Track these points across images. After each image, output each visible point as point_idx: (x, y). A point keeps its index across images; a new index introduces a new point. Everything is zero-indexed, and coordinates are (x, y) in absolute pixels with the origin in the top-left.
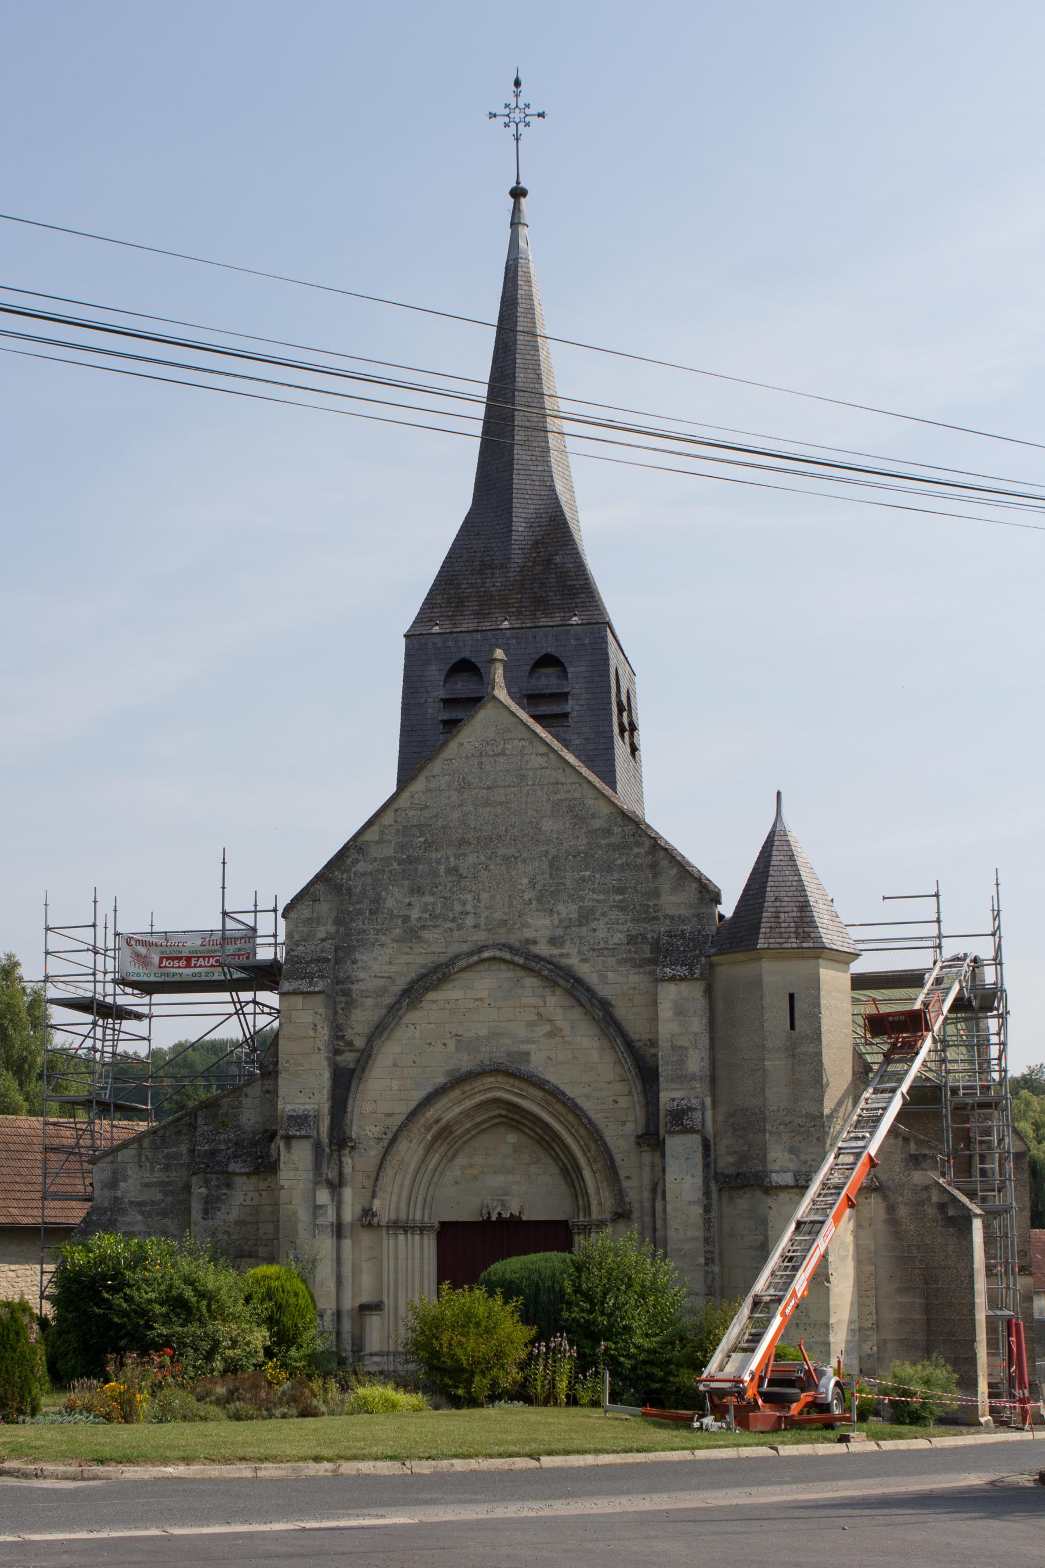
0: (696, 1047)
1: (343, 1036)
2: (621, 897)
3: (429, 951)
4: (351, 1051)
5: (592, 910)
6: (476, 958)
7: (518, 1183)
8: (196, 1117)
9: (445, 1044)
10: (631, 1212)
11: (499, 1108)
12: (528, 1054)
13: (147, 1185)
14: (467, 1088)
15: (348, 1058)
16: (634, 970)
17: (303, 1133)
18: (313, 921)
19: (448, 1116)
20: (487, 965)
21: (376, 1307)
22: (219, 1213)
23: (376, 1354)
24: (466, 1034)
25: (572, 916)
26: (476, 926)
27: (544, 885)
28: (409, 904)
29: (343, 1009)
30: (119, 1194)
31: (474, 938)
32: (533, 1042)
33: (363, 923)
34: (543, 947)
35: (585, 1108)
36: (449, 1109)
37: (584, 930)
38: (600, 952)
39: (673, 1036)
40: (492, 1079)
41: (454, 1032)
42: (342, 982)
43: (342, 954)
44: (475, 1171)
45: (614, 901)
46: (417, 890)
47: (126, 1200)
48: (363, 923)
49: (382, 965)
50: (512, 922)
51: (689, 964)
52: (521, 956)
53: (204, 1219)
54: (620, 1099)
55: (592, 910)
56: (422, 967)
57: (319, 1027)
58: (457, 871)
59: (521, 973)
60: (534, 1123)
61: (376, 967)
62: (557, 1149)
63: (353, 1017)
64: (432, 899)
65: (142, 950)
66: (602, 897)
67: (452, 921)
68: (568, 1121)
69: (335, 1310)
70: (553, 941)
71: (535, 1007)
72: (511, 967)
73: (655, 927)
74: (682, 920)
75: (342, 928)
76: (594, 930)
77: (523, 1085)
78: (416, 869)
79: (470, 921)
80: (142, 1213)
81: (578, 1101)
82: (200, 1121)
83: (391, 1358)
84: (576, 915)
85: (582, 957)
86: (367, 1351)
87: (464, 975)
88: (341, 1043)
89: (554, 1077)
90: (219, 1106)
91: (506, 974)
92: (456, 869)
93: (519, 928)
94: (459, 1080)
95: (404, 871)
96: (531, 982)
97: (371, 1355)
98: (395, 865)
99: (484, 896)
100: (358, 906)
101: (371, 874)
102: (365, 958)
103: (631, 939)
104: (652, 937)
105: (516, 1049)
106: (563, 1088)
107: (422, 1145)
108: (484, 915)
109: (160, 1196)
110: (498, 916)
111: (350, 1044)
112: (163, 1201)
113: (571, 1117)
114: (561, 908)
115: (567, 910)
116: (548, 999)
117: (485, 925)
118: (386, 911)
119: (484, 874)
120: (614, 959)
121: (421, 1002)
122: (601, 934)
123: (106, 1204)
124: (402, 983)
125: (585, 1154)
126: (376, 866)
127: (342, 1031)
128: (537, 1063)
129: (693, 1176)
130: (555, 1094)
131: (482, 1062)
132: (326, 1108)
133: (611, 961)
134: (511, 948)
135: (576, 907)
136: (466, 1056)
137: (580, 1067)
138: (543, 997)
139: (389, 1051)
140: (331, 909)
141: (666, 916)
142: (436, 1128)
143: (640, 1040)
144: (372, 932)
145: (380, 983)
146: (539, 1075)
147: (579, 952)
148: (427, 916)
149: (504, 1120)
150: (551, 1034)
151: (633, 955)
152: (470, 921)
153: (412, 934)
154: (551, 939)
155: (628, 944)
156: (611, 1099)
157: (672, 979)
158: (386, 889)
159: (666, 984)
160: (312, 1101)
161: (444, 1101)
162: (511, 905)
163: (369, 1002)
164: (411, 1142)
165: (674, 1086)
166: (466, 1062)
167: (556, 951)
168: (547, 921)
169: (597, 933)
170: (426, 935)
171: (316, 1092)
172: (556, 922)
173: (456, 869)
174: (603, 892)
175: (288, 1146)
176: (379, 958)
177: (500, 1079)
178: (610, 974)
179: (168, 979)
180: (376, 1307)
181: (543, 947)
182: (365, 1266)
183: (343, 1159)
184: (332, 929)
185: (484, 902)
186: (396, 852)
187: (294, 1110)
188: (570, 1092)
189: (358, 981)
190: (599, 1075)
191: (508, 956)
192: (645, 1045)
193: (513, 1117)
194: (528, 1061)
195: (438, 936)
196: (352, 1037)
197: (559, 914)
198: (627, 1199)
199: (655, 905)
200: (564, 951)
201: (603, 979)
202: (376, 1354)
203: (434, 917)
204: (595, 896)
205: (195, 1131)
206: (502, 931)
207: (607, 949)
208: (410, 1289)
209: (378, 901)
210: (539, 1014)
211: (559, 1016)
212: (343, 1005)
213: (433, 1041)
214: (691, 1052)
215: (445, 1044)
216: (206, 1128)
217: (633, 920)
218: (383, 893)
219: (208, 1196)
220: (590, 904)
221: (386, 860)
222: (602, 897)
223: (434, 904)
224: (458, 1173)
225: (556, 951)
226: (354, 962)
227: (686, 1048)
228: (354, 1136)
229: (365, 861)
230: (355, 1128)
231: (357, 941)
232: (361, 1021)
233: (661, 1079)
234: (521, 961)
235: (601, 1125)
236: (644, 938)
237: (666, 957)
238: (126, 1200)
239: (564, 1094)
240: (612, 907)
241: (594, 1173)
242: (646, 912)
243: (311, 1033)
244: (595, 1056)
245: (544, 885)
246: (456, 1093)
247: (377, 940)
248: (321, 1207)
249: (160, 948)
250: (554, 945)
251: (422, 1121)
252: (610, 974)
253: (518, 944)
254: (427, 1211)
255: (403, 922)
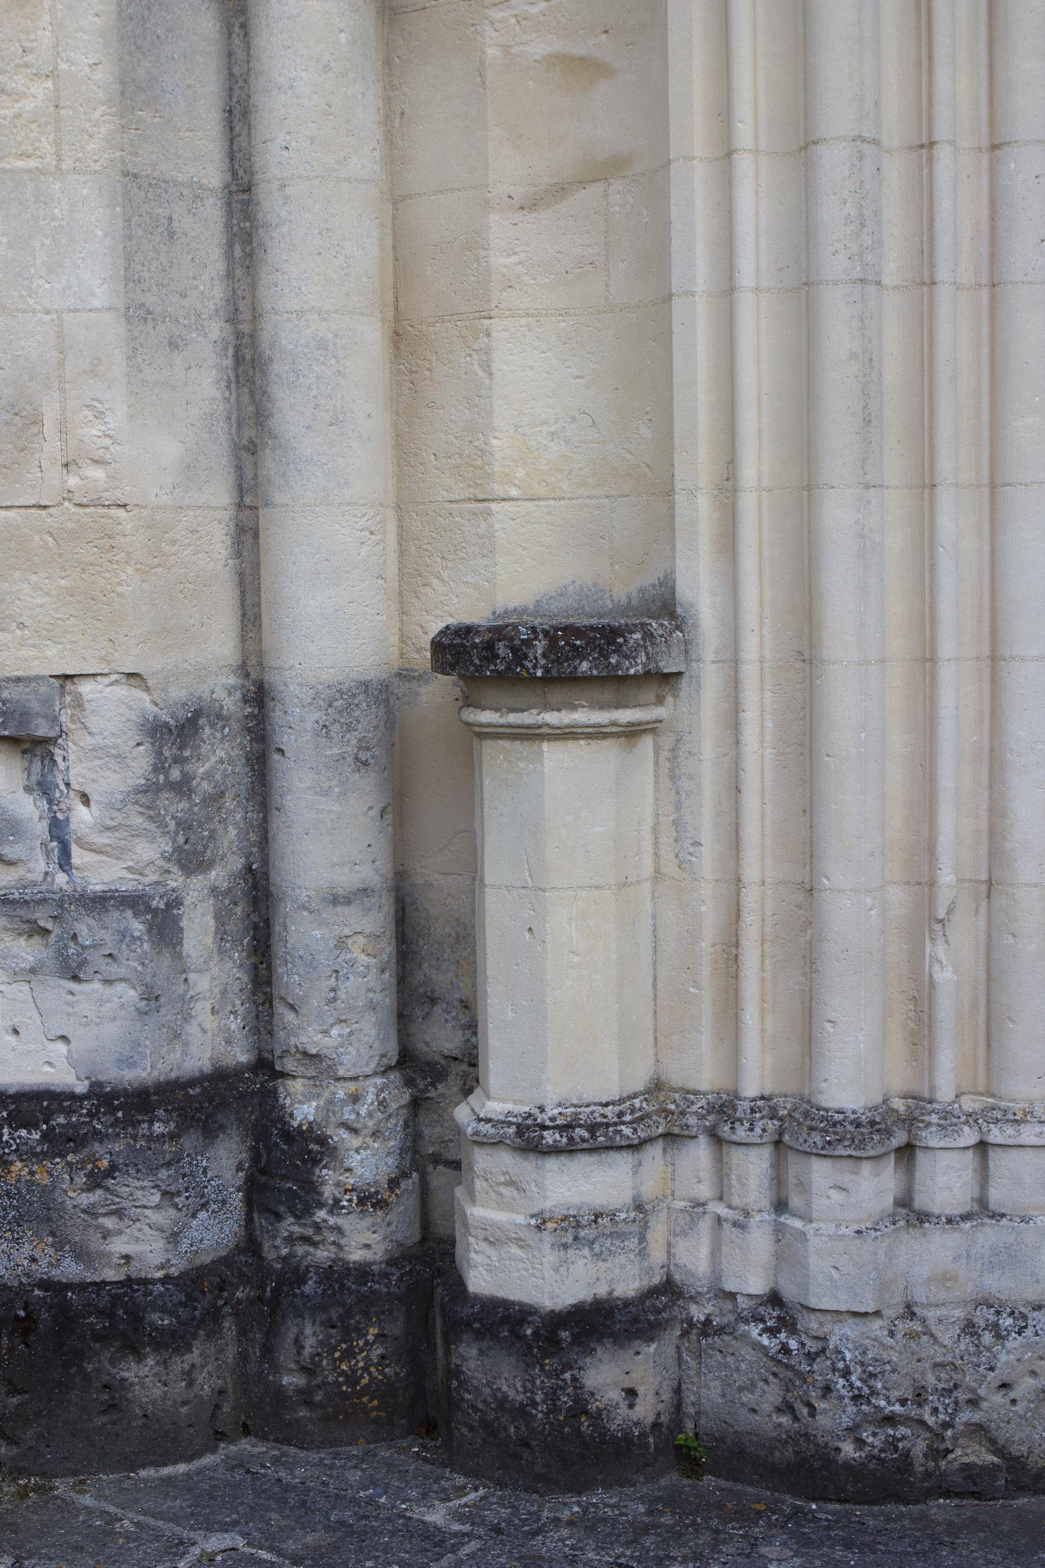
21: (587, 659)
23: (584, 1135)
69: (222, 689)
83: (753, 1167)
86: (500, 1098)
97: (530, 1138)
180: (587, 659)
182: (514, 246)
202: (584, 1135)
208: (956, 460)
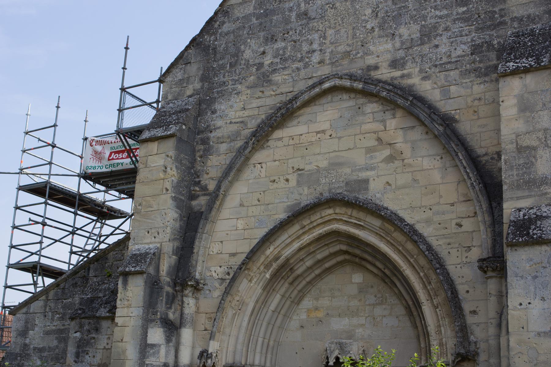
0: (547, 146)
1: (200, 181)
2: (465, 9)
3: (278, 92)
4: (205, 195)
5: (435, 27)
6: (317, 90)
7: (362, 325)
8: (89, 270)
9: (287, 180)
10: (477, 354)
11: (341, 242)
12: (366, 181)
13: (47, 333)
14: (306, 222)
15: (201, 202)
16: (479, 80)
17: (138, 268)
18: (183, 82)
19: (288, 252)
20: (329, 97)
22: (87, 357)
24: (307, 168)
25: (414, 36)
26: (321, 62)
27: (387, 12)
28: (264, 53)
29: (201, 157)
30: (27, 341)
31: (319, 73)
32: (372, 169)
33: (224, 77)
34: (384, 71)
35: (425, 234)
36: (287, 246)
37: (426, 48)
38: (443, 67)
39: (518, 136)
40: (330, 211)
41: (296, 167)
42: (202, 132)
43: (205, 106)
44: (320, 314)
45: (458, 14)
46: (272, 39)
47: (32, 347)
48: (224, 77)
49: (237, 112)
50: (354, 52)
51: (537, 55)
52: (360, 81)
53: (75, 362)
54: (465, 222)
55: (435, 27)
56: (271, 109)
57: (168, 169)
58: (306, 15)
59: (362, 100)
60: (375, 257)
61: (232, 114)
62: (398, 284)
63: (209, 163)
64: (283, 44)
65: (99, 148)
66: (445, 12)
67: (300, 61)
68: (407, 251)
70: (395, 64)
71: (375, 132)
72: (353, 95)
73: (501, 32)
74: (531, 19)
75: (206, 84)
76: (437, 46)
77: (361, 215)
78: (271, 21)
79: (316, 58)
80: (41, 358)
81: (418, 227)
82: (92, 273)
84: (418, 35)
85: (424, 75)
87: (308, 110)
88: (197, 189)
89: (392, 203)
90: (107, 259)
91: (346, 103)
92: (306, 14)
93: (361, 57)
94: (298, 214)
95: (261, 24)
96: (372, 107)
98: (254, 20)
99: (330, 32)
100: (221, 62)
101: (233, 32)
102: (223, 107)
103: (476, 49)
104: (499, 43)
105: (355, 178)
106: (401, 214)
107: (261, 284)
108: (328, 50)
109: (55, 343)
110: (342, 48)
111: (204, 188)
112: (57, 346)
113: (410, 246)
114: (404, 31)
115: (409, 31)
116: (388, 123)
117: (330, 59)
118: (243, 62)
119: (330, 13)
120: (457, 72)
121: (268, 141)
122: (443, 49)
123: (18, 350)
124: (253, 125)
125: (425, 287)
126: (238, 24)
127: (198, 177)
128: (377, 191)
129: (543, 299)
130: (391, 220)
131: (321, 194)
132: (168, 248)
133: (454, 74)
134: (352, 77)
135: (418, 27)
136: (306, 191)
137: (420, 189)
138: (383, 121)
139: (239, 191)
140: (199, 69)
141: (513, 20)
142: (275, 266)
143: (486, 154)
144: (230, 83)
145: (234, 127)
146: (378, 202)
147: (421, 71)
148: (278, 60)
149: (347, 257)
150: (391, 159)
151: (477, 65)
152: (316, 58)
153: (265, 79)
154: (393, 62)
155: (472, 54)
156: (454, 222)
157: (515, 72)
158: (245, 43)
159: (508, 79)
160: (157, 240)
161: (284, 237)
162: (354, 36)
163: (223, 147)
164: (250, 281)
165: (520, 193)
166: (306, 196)
167: (398, 73)
168: (389, 46)
169: (440, 49)
170: (277, 78)
171: (161, 231)
172: (398, 45)
173: (306, 14)
174: (445, 7)
175: (125, 283)
176: (235, 105)
177: (338, 211)
178: (453, 88)
179: (114, 169)
181: (384, 71)
183: (185, 299)
184: (198, 85)
185: (329, 39)
186: (255, 8)
187: (139, 250)
188: (409, 218)
189: (215, 129)
190: (441, 197)
191: (347, 83)
192: (492, 159)
193: (356, 254)
194: (367, 189)
195: (286, 77)
196: (207, 182)
197: (400, 36)
198: (472, 338)
199: (501, 10)
200: (405, 72)
201: (446, 95)
203: (284, 60)
204: (438, 13)
205: (87, 283)
206: (345, 62)
207: (449, 62)
209: (237, 54)
210: (379, 140)
211: (399, 138)
212: (201, 153)
213: (276, 178)
214: (540, 152)
215: (287, 180)
216: (95, 279)
217: (477, 29)
218: (242, 47)
219: (80, 340)
220: (433, 21)
221: (247, 18)
222: (445, 12)
223: (285, 48)
224: (304, 316)
225: (398, 73)
226: (214, 112)
227: (535, 149)
228: (197, 276)
229: (229, 22)
230: (199, 268)
231: (218, 92)
232: (214, 166)
233: (505, 187)
234: (360, 86)
235: (443, 252)
236: (490, 44)
237: (510, 54)
238: (32, 347)
239: (402, 220)
240: (454, 20)
241: (436, 307)
242: (492, 18)
243: (162, 175)
244: (437, 176)
245: (387, 12)
246: (295, 229)
247: (234, 89)
248: (153, 346)
249: (111, 145)
250: (395, 68)
251: (262, 259)
252: (453, 88)
253: (359, 72)
254: (269, 356)
255: (257, 70)
